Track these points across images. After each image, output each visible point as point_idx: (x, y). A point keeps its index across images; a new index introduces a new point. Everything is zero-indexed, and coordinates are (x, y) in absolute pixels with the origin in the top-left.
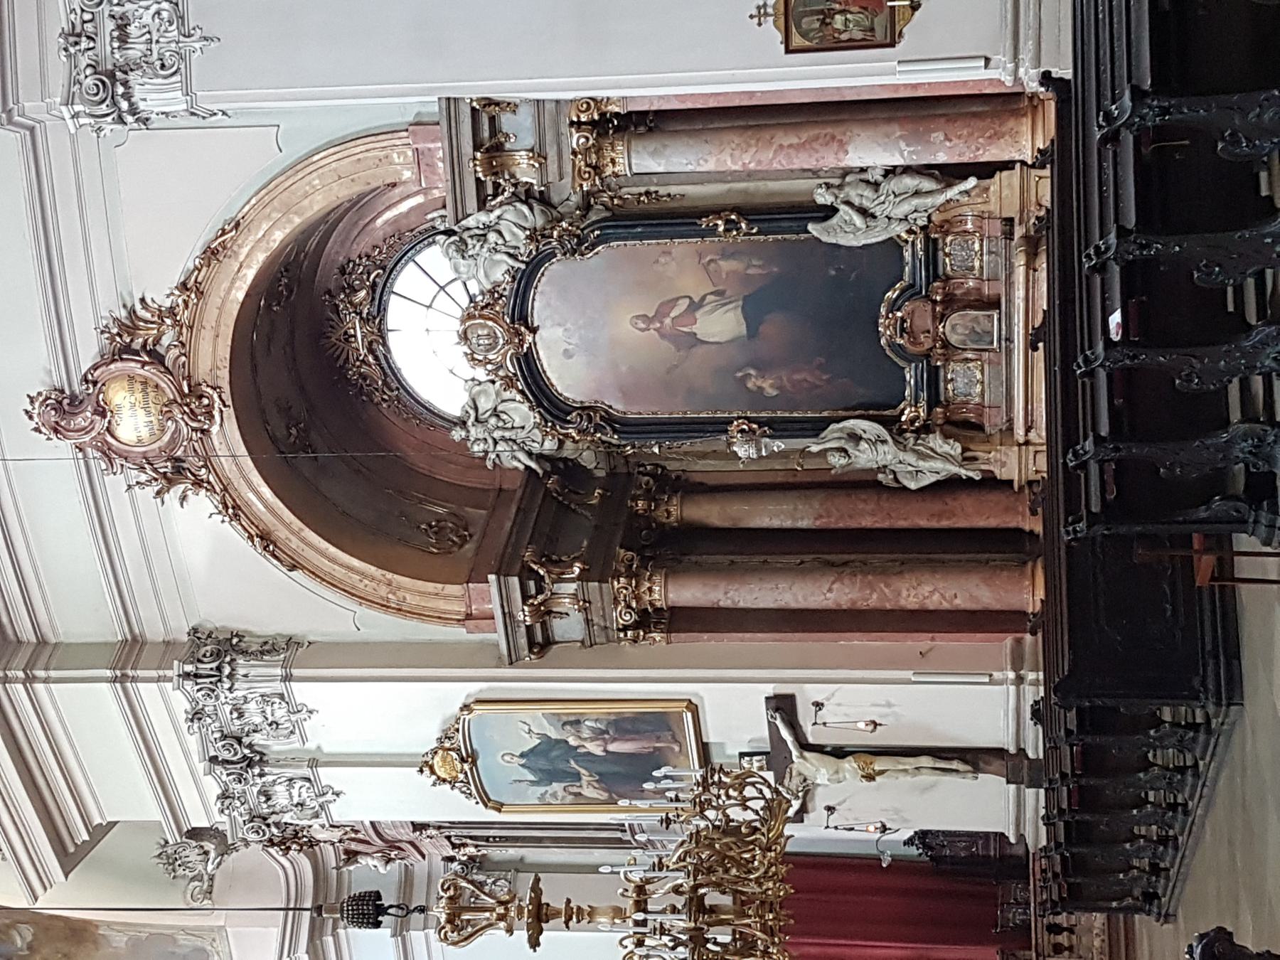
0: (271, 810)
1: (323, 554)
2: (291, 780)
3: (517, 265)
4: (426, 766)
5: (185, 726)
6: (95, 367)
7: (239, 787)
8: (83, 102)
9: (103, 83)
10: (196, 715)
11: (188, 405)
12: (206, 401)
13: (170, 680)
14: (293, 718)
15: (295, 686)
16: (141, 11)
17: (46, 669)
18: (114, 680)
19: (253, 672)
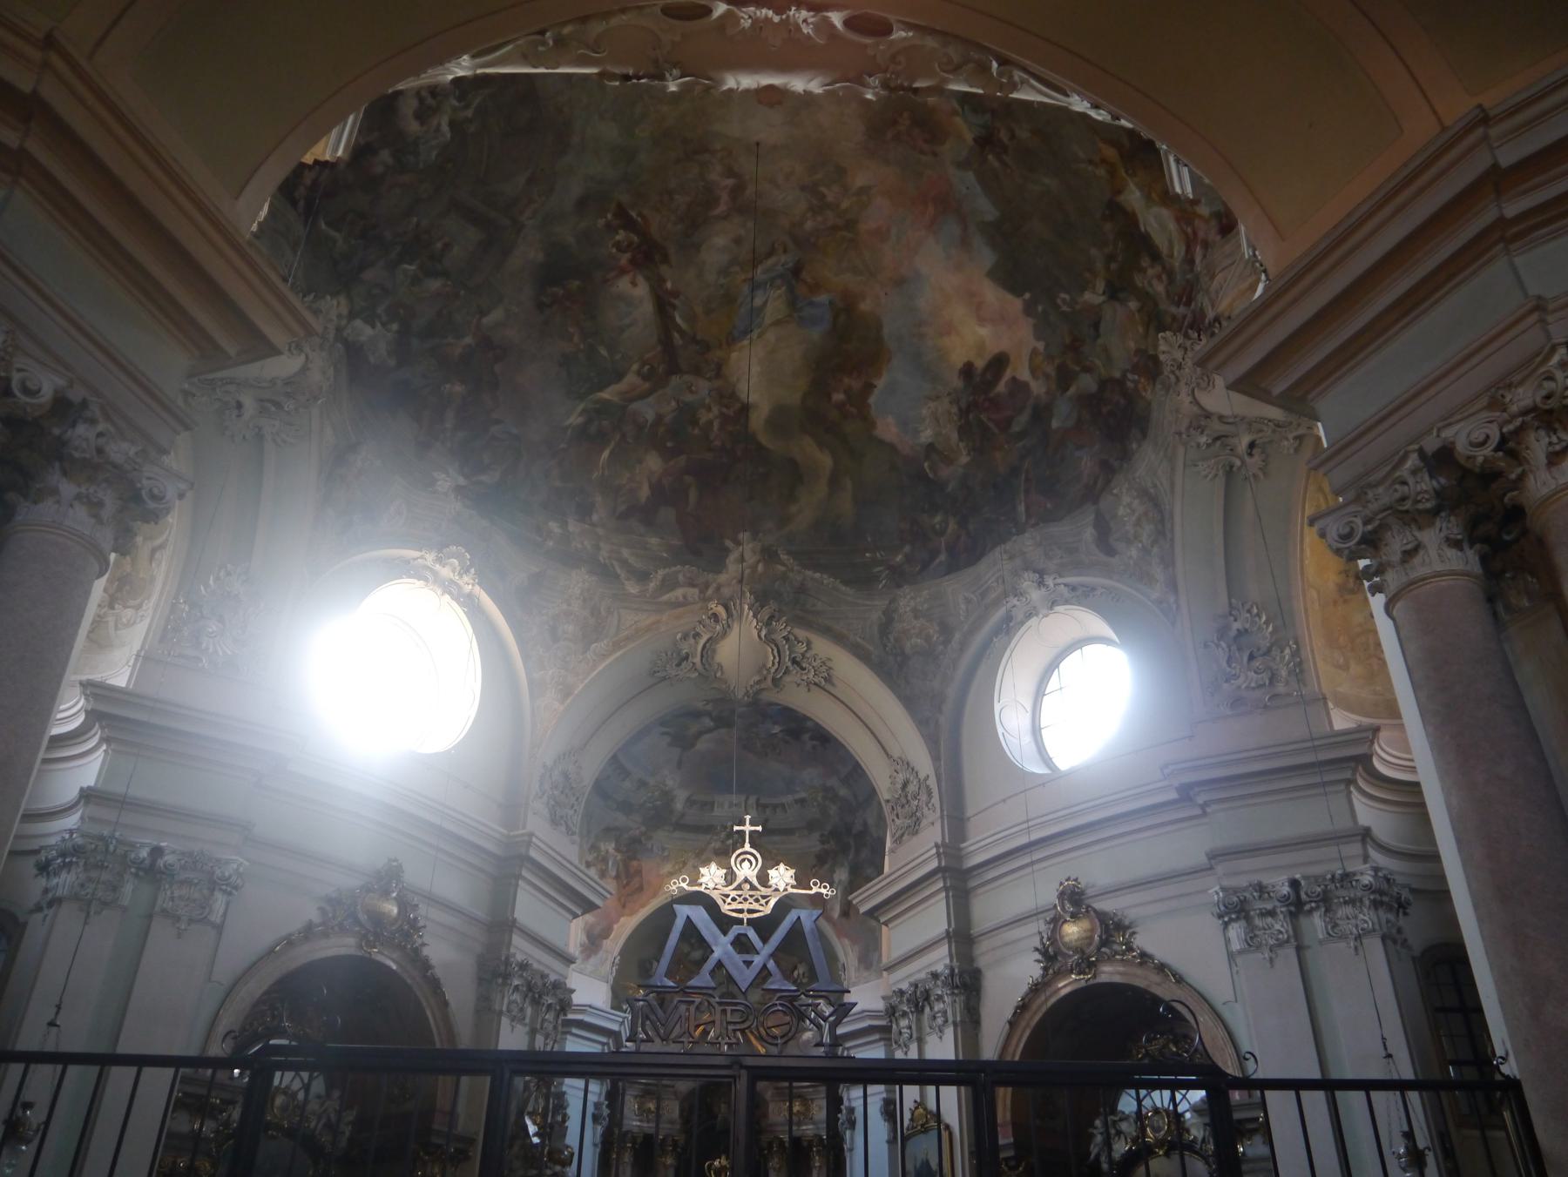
1: (1019, 1040)
2: (910, 1028)
3: (1199, 1142)
5: (929, 970)
6: (1095, 911)
7: (905, 999)
8: (1224, 897)
9: (1236, 906)
10: (935, 976)
11: (1083, 961)
12: (1087, 970)
13: (951, 960)
14: (937, 1029)
15: (952, 1028)
16: (1280, 923)
17: (953, 896)
18: (947, 932)
19: (957, 1006)
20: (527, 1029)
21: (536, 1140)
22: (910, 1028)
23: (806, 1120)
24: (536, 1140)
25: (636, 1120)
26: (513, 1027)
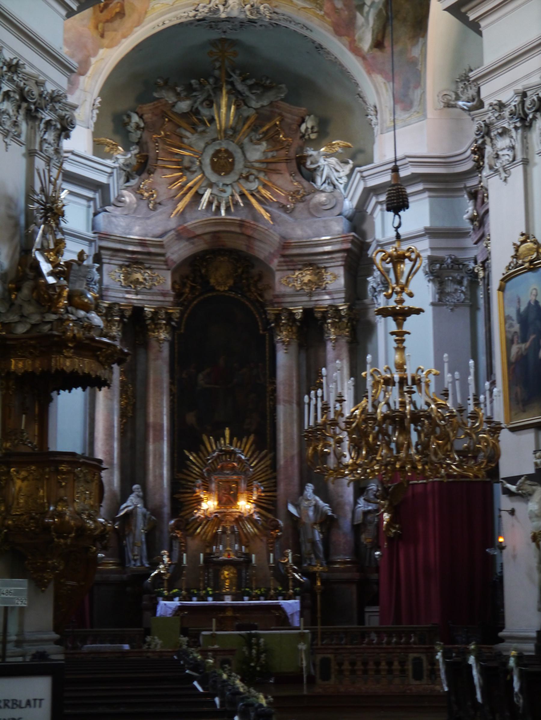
0: (493, 138)
2: (513, 148)
4: (526, 237)
7: (506, 113)
20: (23, 149)
21: (51, 280)
22: (513, 148)
23: (319, 290)
24: (51, 280)
25: (121, 292)
26: (7, 144)
